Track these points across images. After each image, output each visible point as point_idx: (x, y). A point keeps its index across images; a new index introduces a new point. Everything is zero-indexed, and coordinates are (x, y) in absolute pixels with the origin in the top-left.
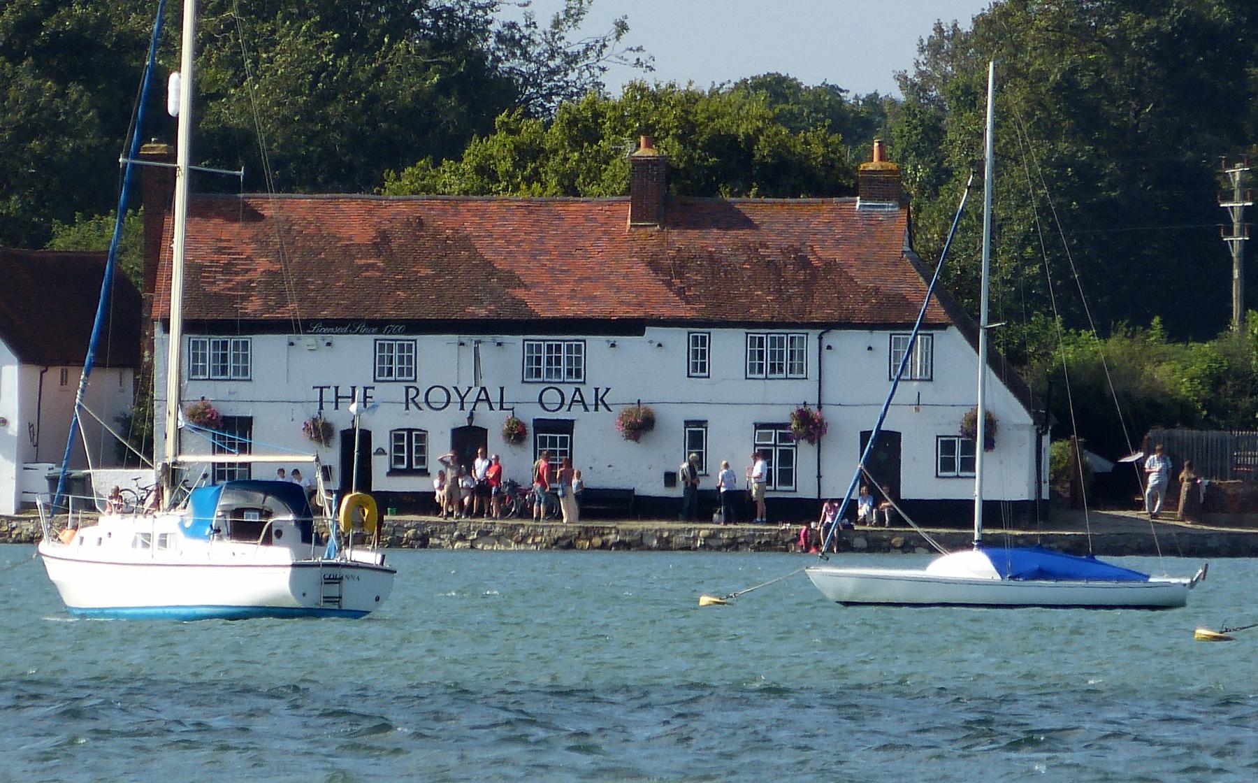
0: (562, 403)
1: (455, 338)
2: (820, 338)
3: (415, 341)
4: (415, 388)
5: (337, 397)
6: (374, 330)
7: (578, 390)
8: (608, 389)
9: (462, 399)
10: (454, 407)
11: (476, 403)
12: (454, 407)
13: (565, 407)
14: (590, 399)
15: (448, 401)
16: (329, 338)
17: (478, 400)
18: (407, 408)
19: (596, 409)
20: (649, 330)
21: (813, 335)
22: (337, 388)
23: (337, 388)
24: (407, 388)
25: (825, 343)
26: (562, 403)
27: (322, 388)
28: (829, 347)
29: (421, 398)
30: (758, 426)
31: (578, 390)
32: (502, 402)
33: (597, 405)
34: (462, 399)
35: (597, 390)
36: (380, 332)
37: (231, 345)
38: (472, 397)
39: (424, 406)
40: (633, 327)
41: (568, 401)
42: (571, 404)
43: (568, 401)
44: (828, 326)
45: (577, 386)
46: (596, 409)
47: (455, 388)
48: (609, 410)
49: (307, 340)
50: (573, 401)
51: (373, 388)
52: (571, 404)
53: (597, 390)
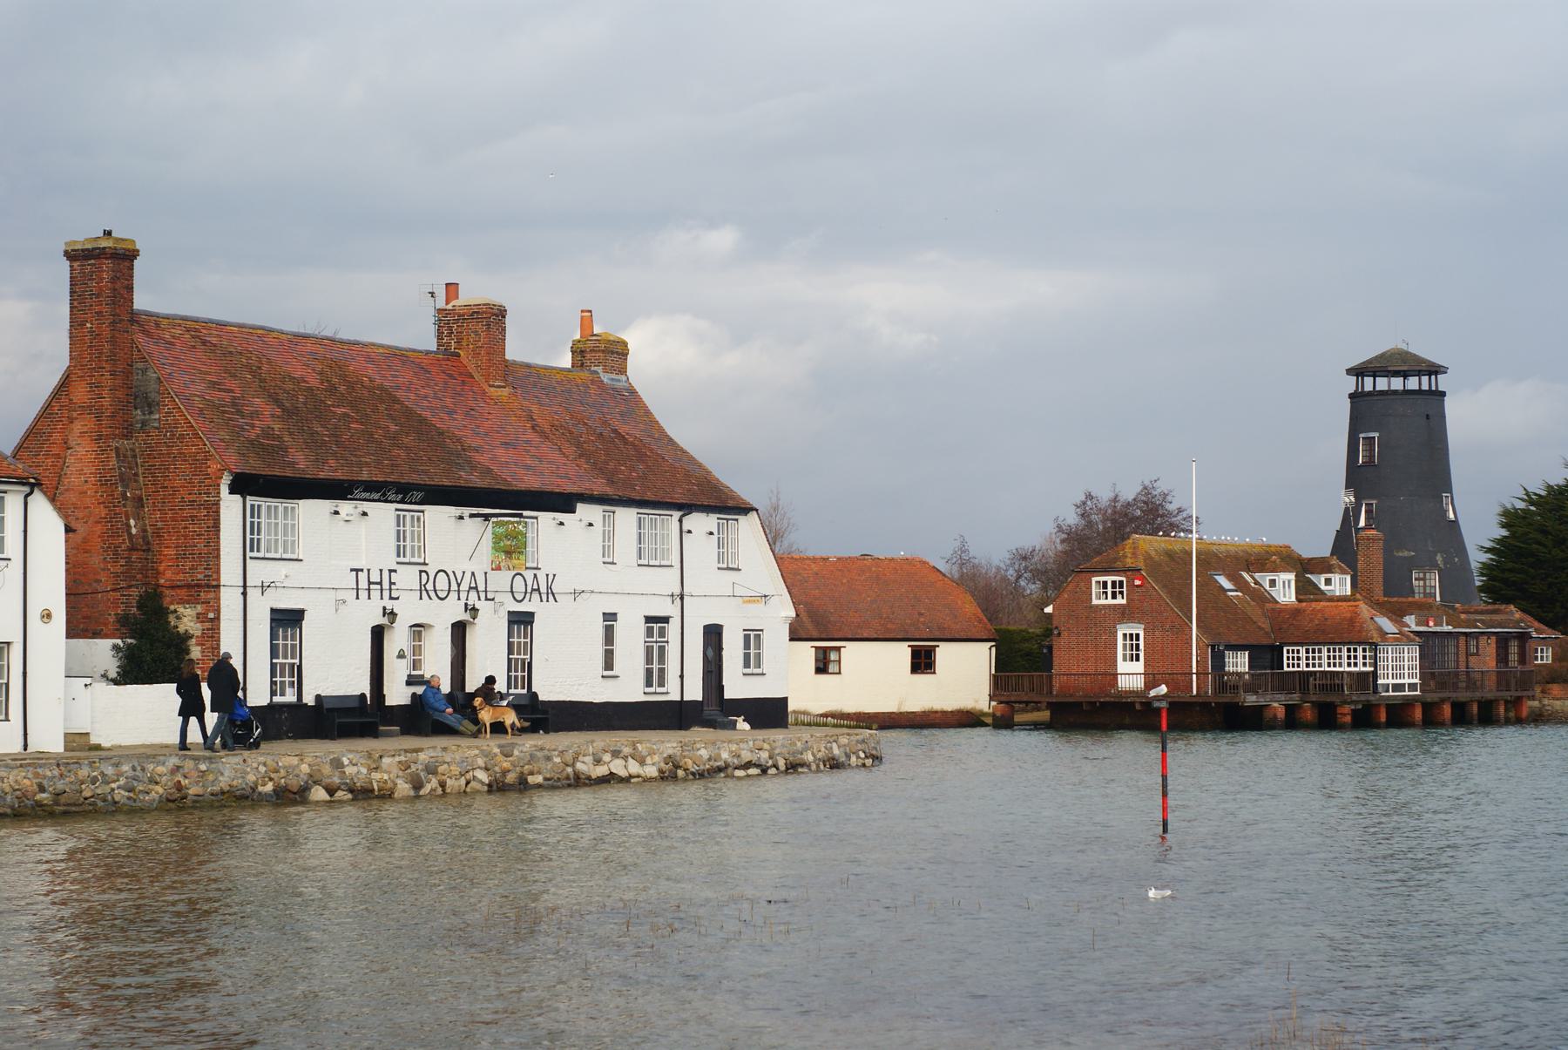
0: (526, 593)
1: (453, 511)
2: (680, 521)
3: (423, 512)
4: (425, 572)
5: (370, 583)
6: (400, 496)
7: (535, 575)
8: (554, 575)
9: (459, 585)
10: (454, 595)
11: (468, 591)
12: (454, 595)
13: (528, 595)
14: (543, 589)
15: (449, 591)
16: (366, 506)
17: (470, 588)
18: (421, 598)
19: (548, 601)
20: (580, 507)
21: (677, 514)
22: (369, 570)
23: (369, 570)
24: (421, 572)
25: (685, 528)
26: (526, 593)
27: (357, 571)
28: (689, 532)
29: (430, 586)
30: (649, 619)
31: (535, 575)
32: (486, 591)
33: (548, 593)
34: (459, 585)
35: (547, 575)
36: (402, 502)
37: (281, 509)
38: (465, 586)
39: (432, 594)
40: (563, 503)
41: (529, 590)
42: (531, 593)
43: (529, 590)
44: (687, 508)
45: (535, 571)
46: (548, 601)
47: (454, 572)
48: (556, 601)
49: (346, 507)
50: (533, 590)
51: (395, 571)
52: (531, 593)
53: (547, 575)
